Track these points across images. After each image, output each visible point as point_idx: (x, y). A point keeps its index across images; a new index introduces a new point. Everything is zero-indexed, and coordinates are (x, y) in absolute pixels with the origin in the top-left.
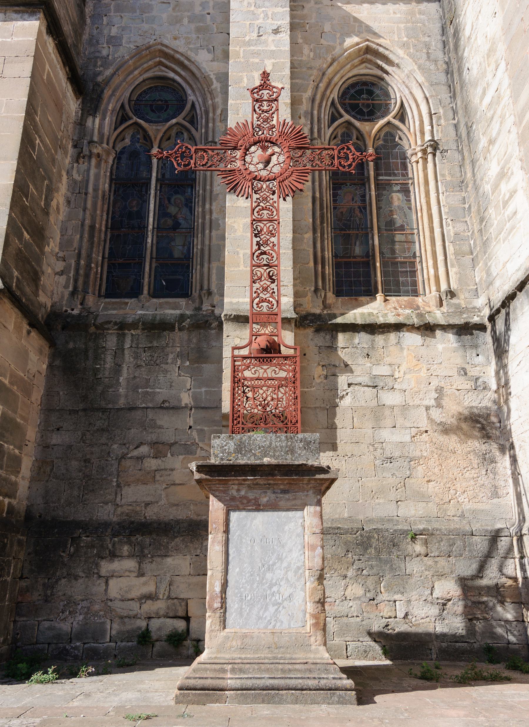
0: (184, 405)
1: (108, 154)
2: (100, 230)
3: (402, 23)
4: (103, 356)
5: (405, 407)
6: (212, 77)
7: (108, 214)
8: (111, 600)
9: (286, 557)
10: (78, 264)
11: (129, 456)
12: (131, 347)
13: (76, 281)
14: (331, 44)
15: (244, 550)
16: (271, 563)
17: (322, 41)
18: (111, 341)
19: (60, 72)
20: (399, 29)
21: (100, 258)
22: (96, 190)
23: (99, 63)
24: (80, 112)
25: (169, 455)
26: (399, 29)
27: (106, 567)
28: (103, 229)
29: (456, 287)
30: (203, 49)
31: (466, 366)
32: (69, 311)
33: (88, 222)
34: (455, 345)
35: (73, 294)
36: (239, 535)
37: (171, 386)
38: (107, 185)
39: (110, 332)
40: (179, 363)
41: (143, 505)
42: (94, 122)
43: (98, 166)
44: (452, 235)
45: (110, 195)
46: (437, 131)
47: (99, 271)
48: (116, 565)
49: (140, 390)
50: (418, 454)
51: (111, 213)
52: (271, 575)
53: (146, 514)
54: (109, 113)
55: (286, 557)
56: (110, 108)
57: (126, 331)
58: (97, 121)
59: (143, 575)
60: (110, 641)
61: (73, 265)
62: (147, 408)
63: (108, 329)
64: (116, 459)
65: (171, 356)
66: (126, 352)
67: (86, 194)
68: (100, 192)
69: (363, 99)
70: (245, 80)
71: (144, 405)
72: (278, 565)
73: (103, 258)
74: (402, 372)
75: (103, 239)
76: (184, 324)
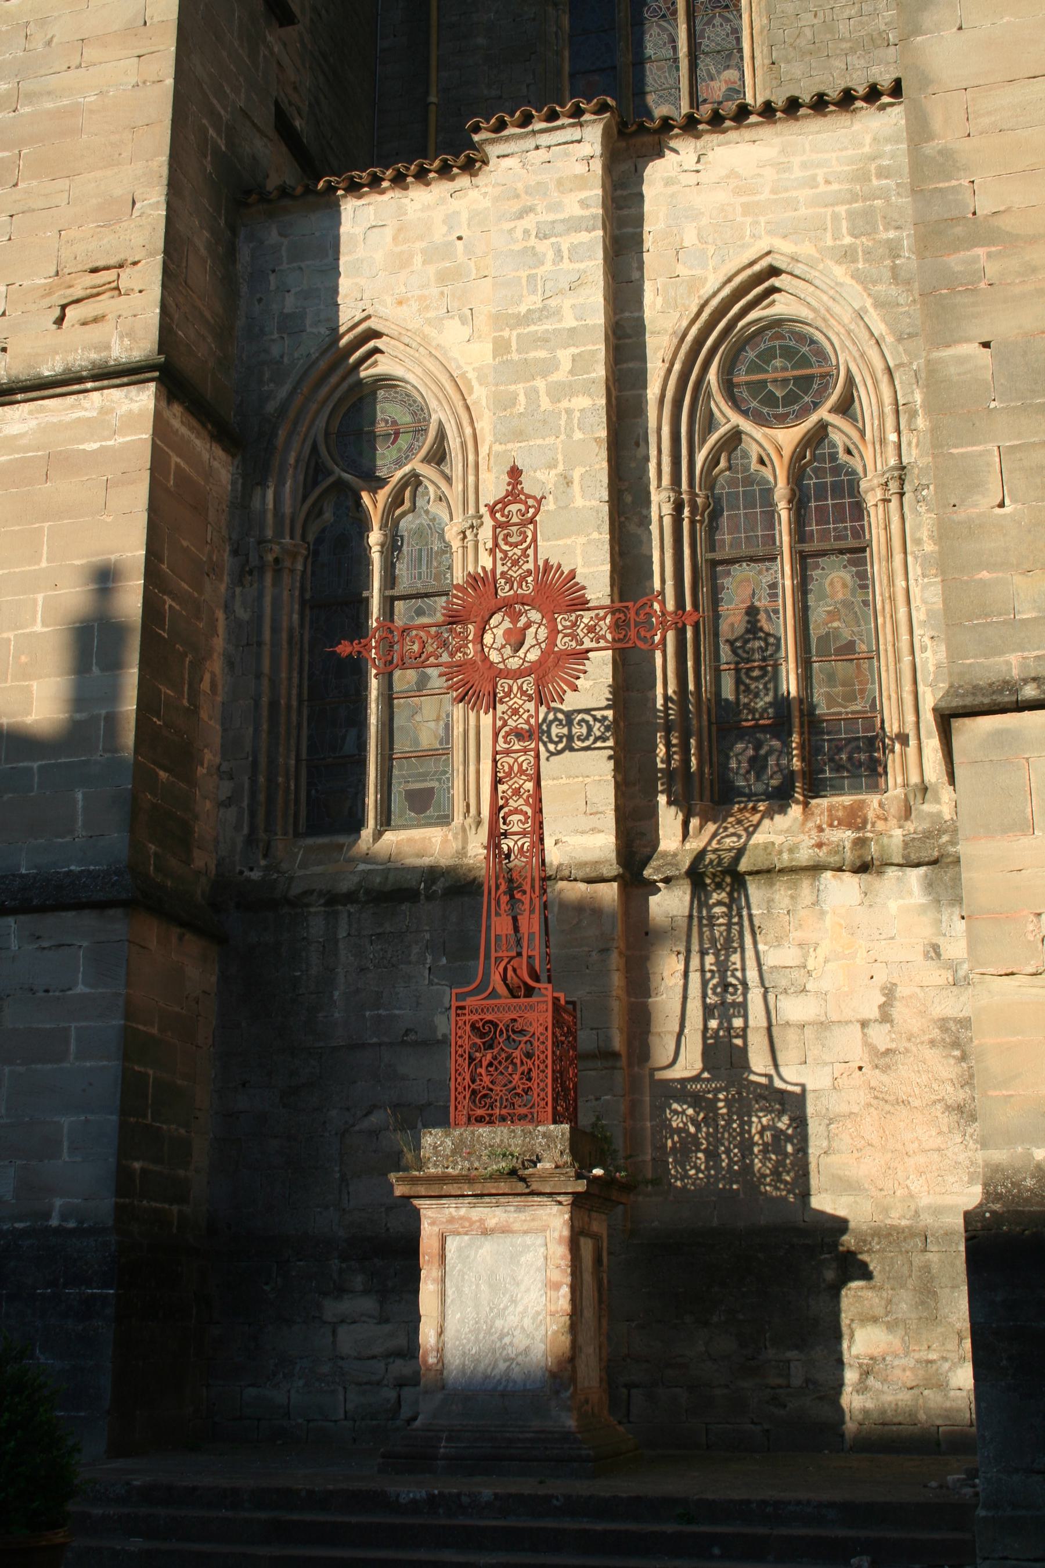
0: (440, 1038)
1: (294, 556)
2: (289, 707)
3: (842, 203)
4: (304, 954)
5: (823, 1025)
6: (471, 375)
7: (301, 673)
8: (342, 1358)
9: (522, 1298)
10: (253, 781)
11: (357, 1128)
12: (349, 934)
13: (253, 814)
14: (698, 272)
15: (466, 1290)
16: (502, 1306)
17: (681, 270)
18: (316, 927)
19: (198, 442)
20: (836, 217)
21: (293, 762)
22: (275, 630)
23: (267, 376)
24: (240, 481)
25: (420, 1125)
26: (836, 217)
27: (332, 1308)
28: (295, 703)
29: (933, 780)
30: (452, 318)
31: (940, 941)
32: (247, 873)
33: (265, 700)
34: (923, 900)
35: (251, 840)
36: (460, 1271)
37: (418, 1004)
38: (296, 617)
39: (313, 910)
40: (429, 961)
41: (383, 1209)
42: (264, 496)
43: (277, 582)
44: (932, 669)
45: (302, 635)
46: (909, 444)
47: (293, 787)
48: (346, 1306)
49: (368, 1013)
50: (844, 1108)
51: (306, 668)
52: (502, 1322)
53: (389, 1225)
54: (291, 471)
55: (522, 1298)
56: (292, 460)
57: (340, 908)
58: (270, 494)
59: (387, 1321)
60: (346, 1418)
61: (246, 786)
62: (380, 1045)
63: (308, 905)
64: (336, 1134)
65: (415, 950)
66: (341, 945)
67: (260, 644)
68: (284, 636)
69: (775, 370)
70: (522, 398)
71: (375, 1040)
72: (511, 1309)
73: (298, 760)
74: (821, 959)
75: (295, 723)
76: (434, 888)
